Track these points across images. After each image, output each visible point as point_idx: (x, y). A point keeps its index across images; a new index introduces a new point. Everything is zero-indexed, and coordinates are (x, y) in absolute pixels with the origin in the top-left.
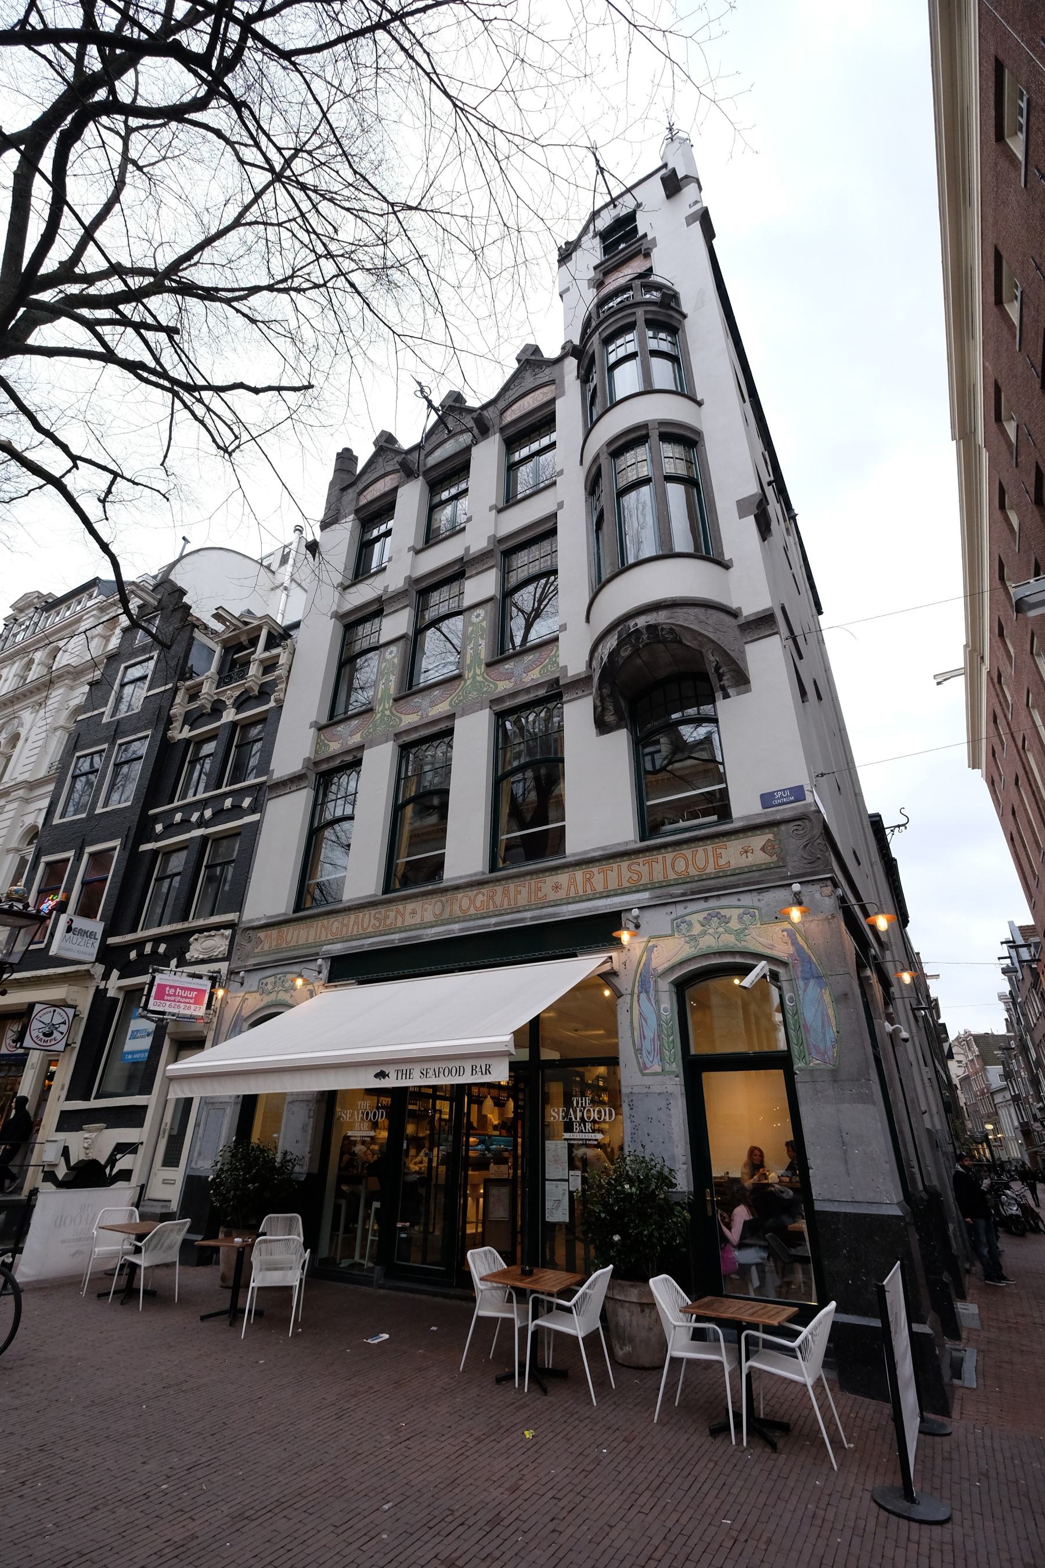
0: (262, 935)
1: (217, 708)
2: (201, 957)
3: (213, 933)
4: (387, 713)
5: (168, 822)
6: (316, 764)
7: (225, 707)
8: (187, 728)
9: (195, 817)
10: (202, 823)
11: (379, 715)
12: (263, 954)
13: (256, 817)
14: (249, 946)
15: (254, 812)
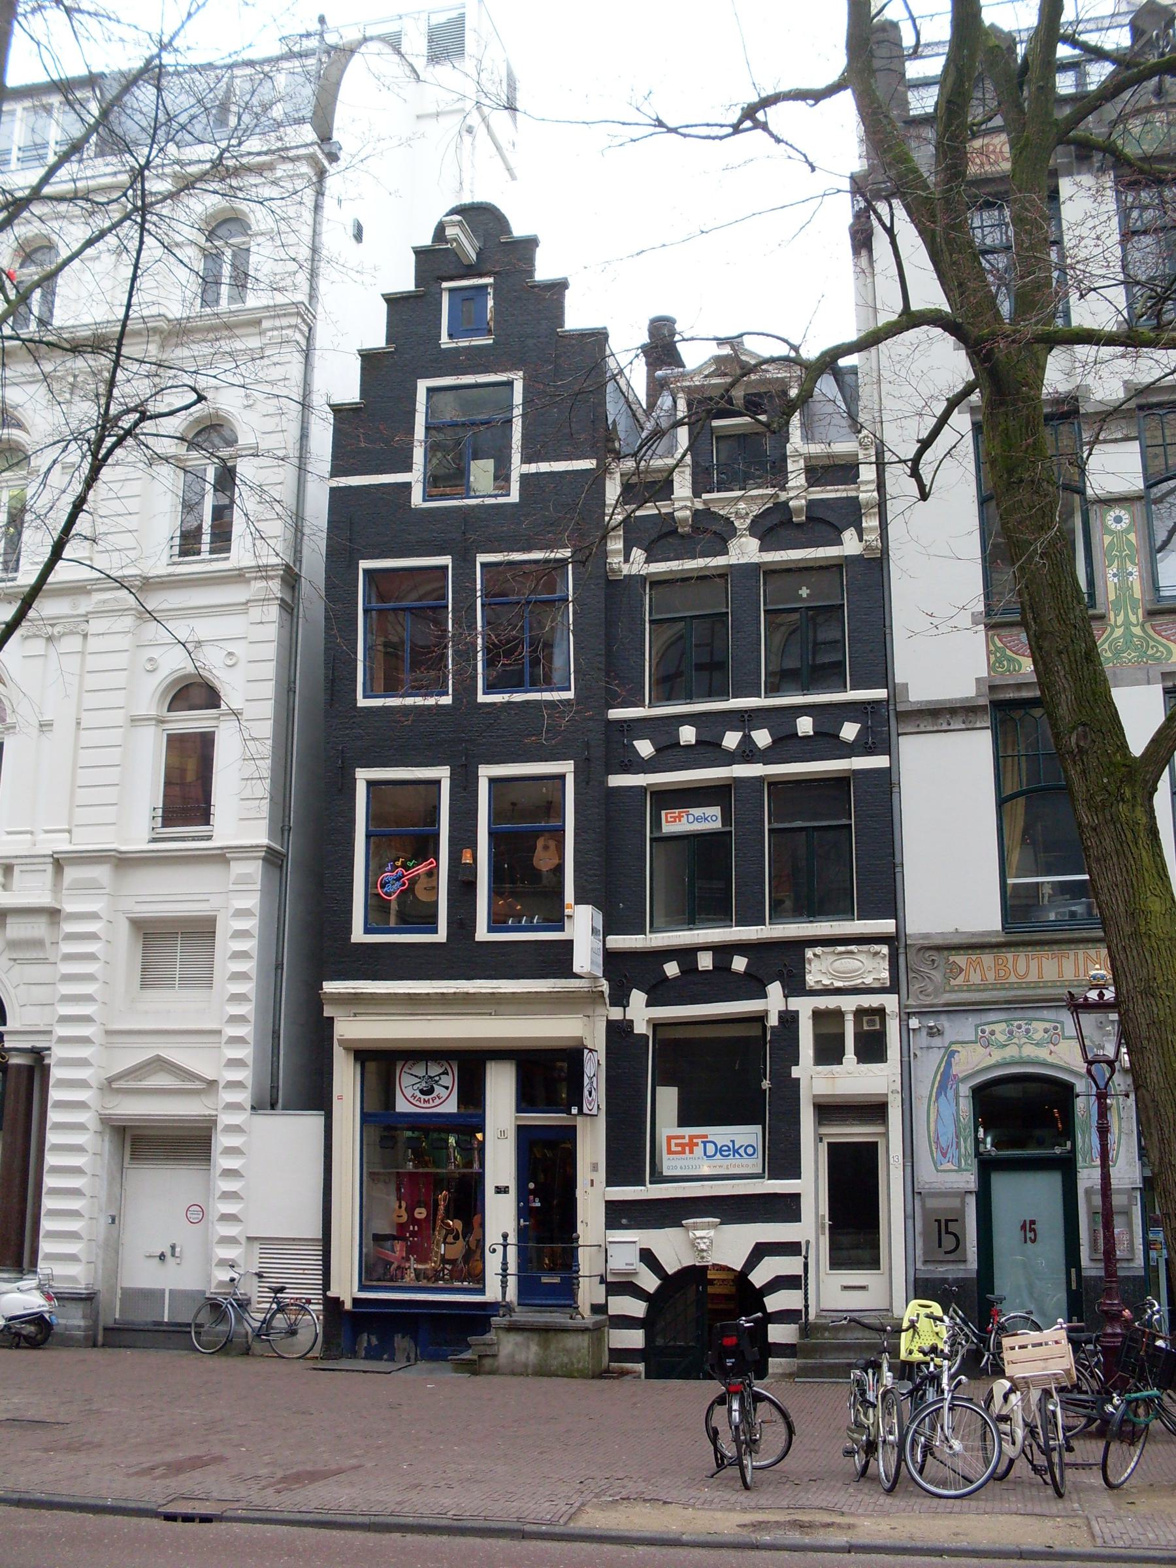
0: (961, 960)
1: (712, 532)
2: (826, 982)
3: (853, 948)
4: (1137, 631)
5: (666, 741)
6: (992, 688)
7: (733, 532)
8: (638, 554)
9: (731, 740)
10: (747, 753)
11: (1119, 632)
12: (970, 988)
13: (880, 762)
14: (937, 976)
15: (870, 751)
